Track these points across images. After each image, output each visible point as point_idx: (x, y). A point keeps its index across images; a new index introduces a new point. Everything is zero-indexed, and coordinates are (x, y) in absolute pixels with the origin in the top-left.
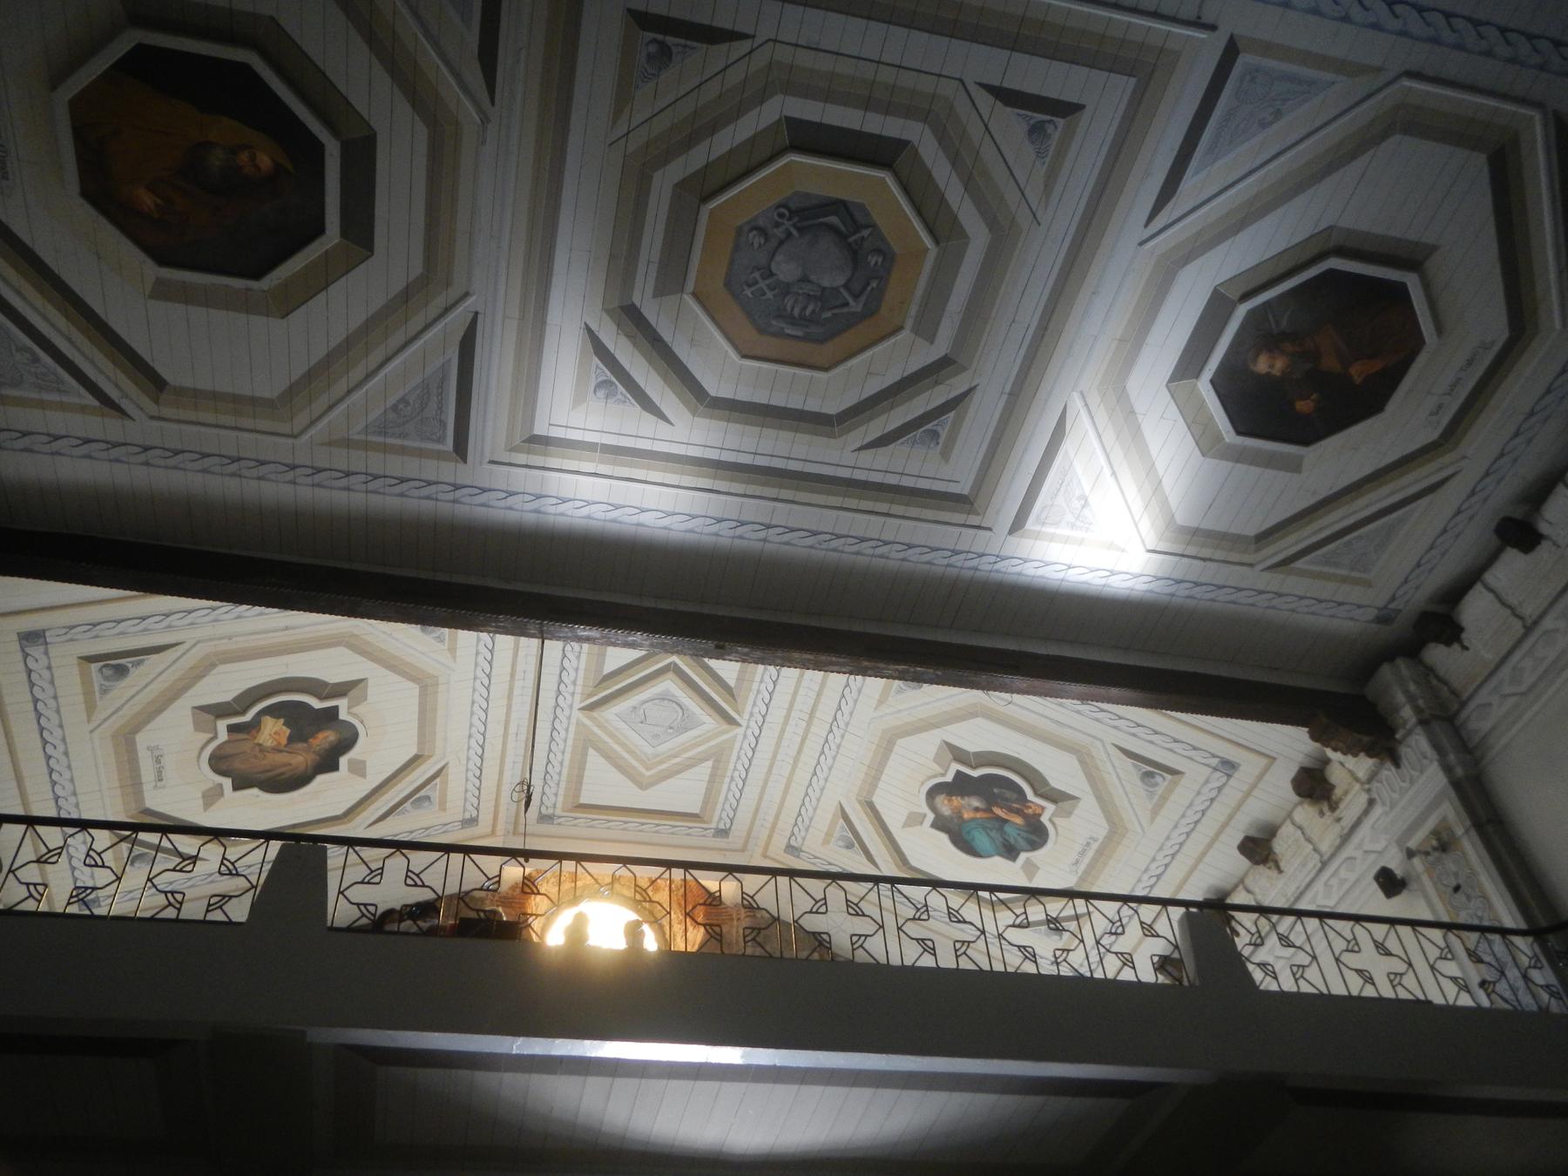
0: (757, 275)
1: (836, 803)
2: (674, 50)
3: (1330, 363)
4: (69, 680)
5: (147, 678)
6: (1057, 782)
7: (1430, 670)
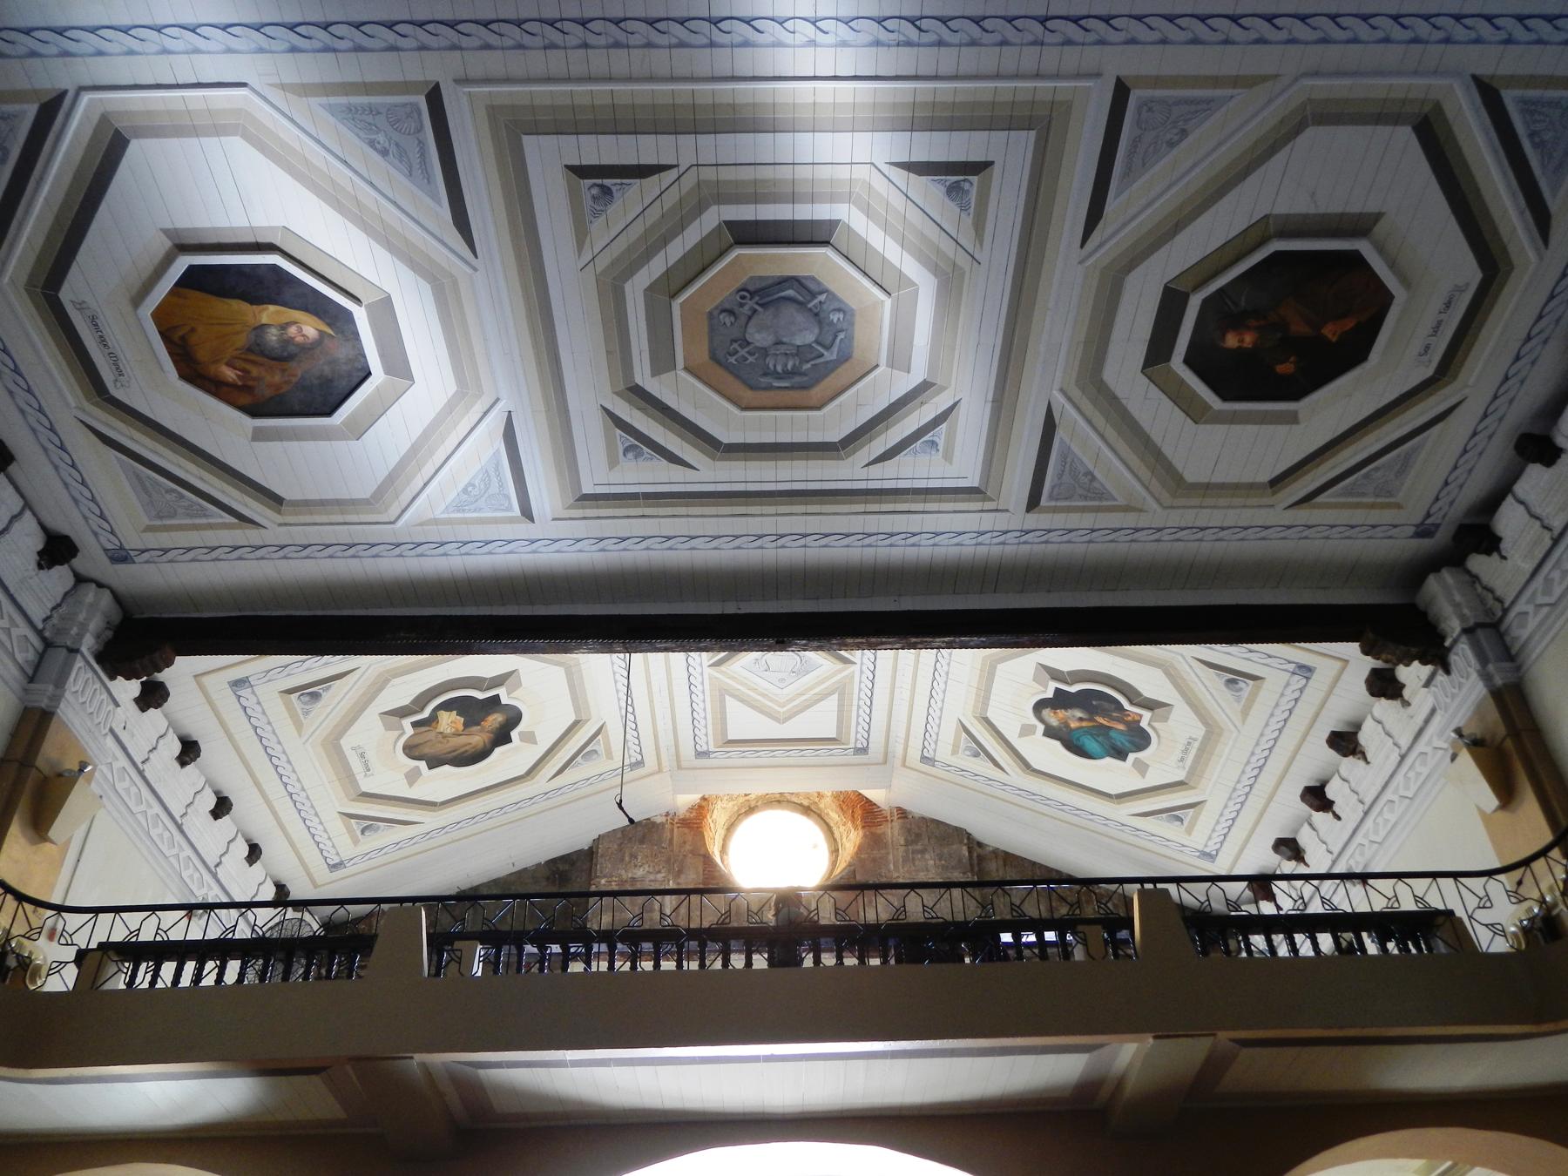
0: (735, 345)
1: (955, 721)
2: (614, 189)
3: (1299, 328)
4: (276, 708)
5: (337, 699)
6: (1148, 692)
7: (1475, 578)
